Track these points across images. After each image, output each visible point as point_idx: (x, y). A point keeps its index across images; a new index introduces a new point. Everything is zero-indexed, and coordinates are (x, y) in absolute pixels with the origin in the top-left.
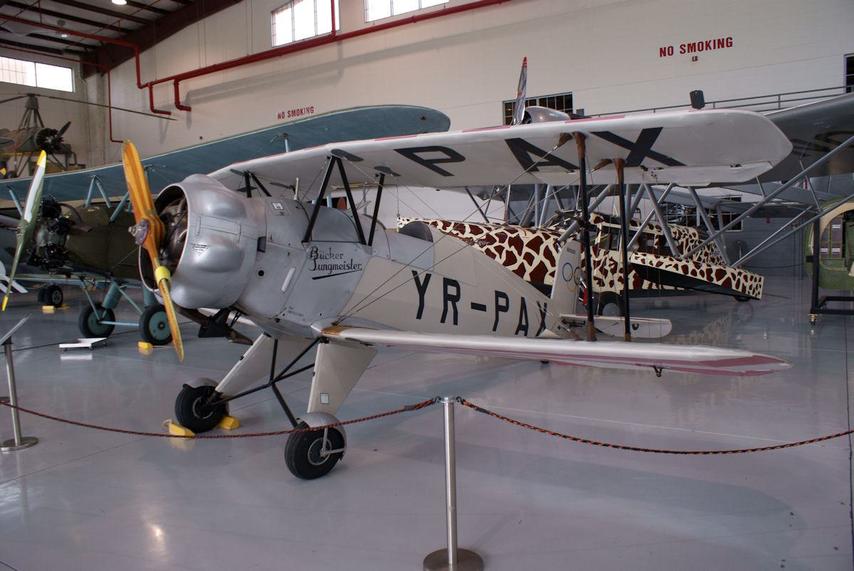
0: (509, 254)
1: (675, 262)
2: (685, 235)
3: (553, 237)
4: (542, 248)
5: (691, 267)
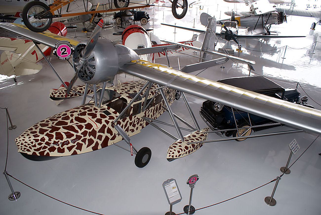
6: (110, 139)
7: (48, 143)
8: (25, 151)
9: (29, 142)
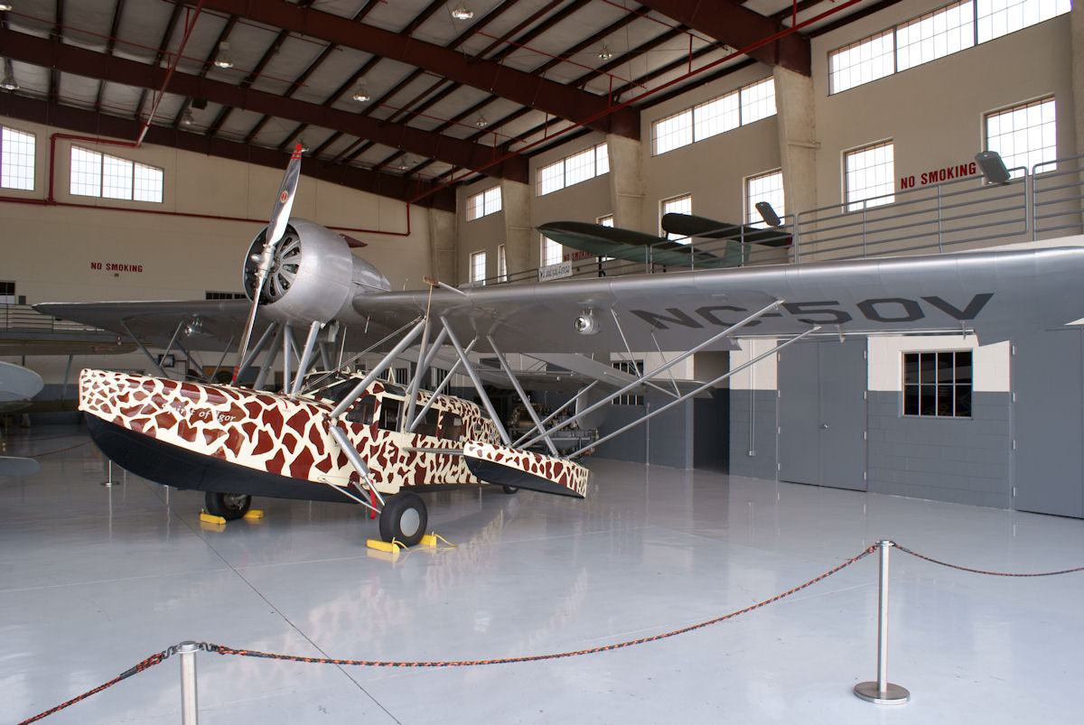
0: (263, 435)
2: (469, 411)
6: (314, 464)
9: (114, 385)
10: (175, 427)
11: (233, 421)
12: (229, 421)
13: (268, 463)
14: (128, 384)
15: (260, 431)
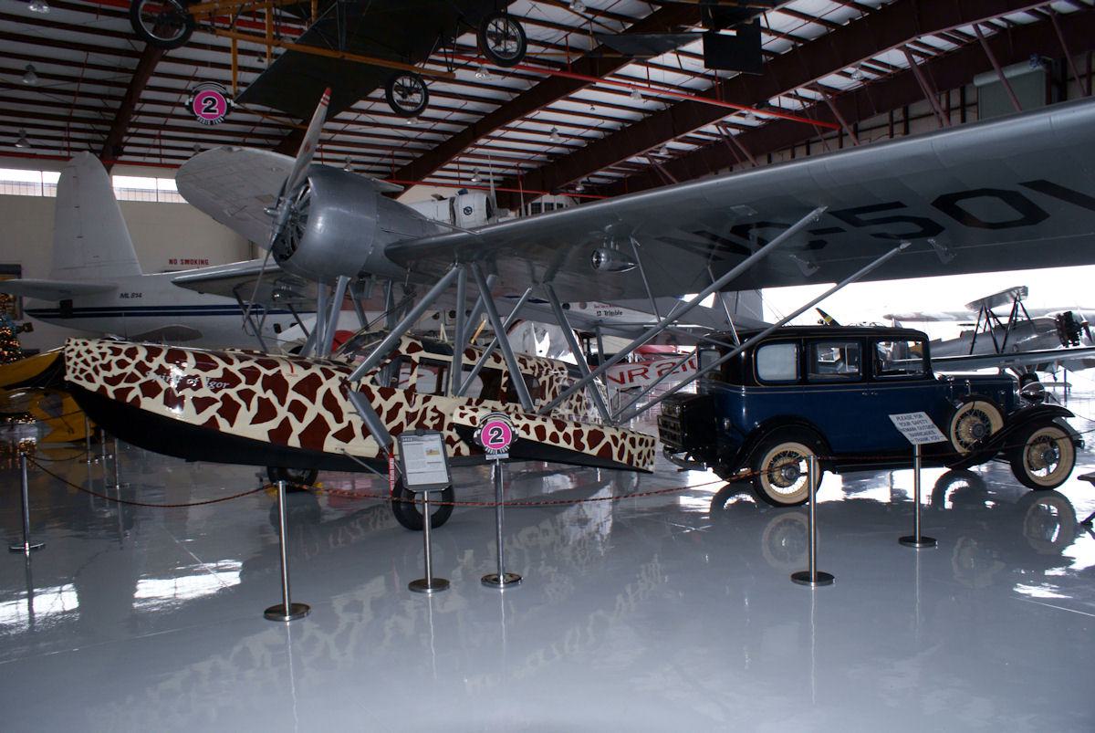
0: (264, 403)
1: (525, 421)
3: (338, 374)
4: (321, 392)
5: (550, 428)
7: (142, 367)
8: (81, 379)
9: (96, 354)
10: (161, 397)
11: (227, 387)
12: (221, 388)
13: (271, 432)
14: (110, 352)
15: (259, 398)
